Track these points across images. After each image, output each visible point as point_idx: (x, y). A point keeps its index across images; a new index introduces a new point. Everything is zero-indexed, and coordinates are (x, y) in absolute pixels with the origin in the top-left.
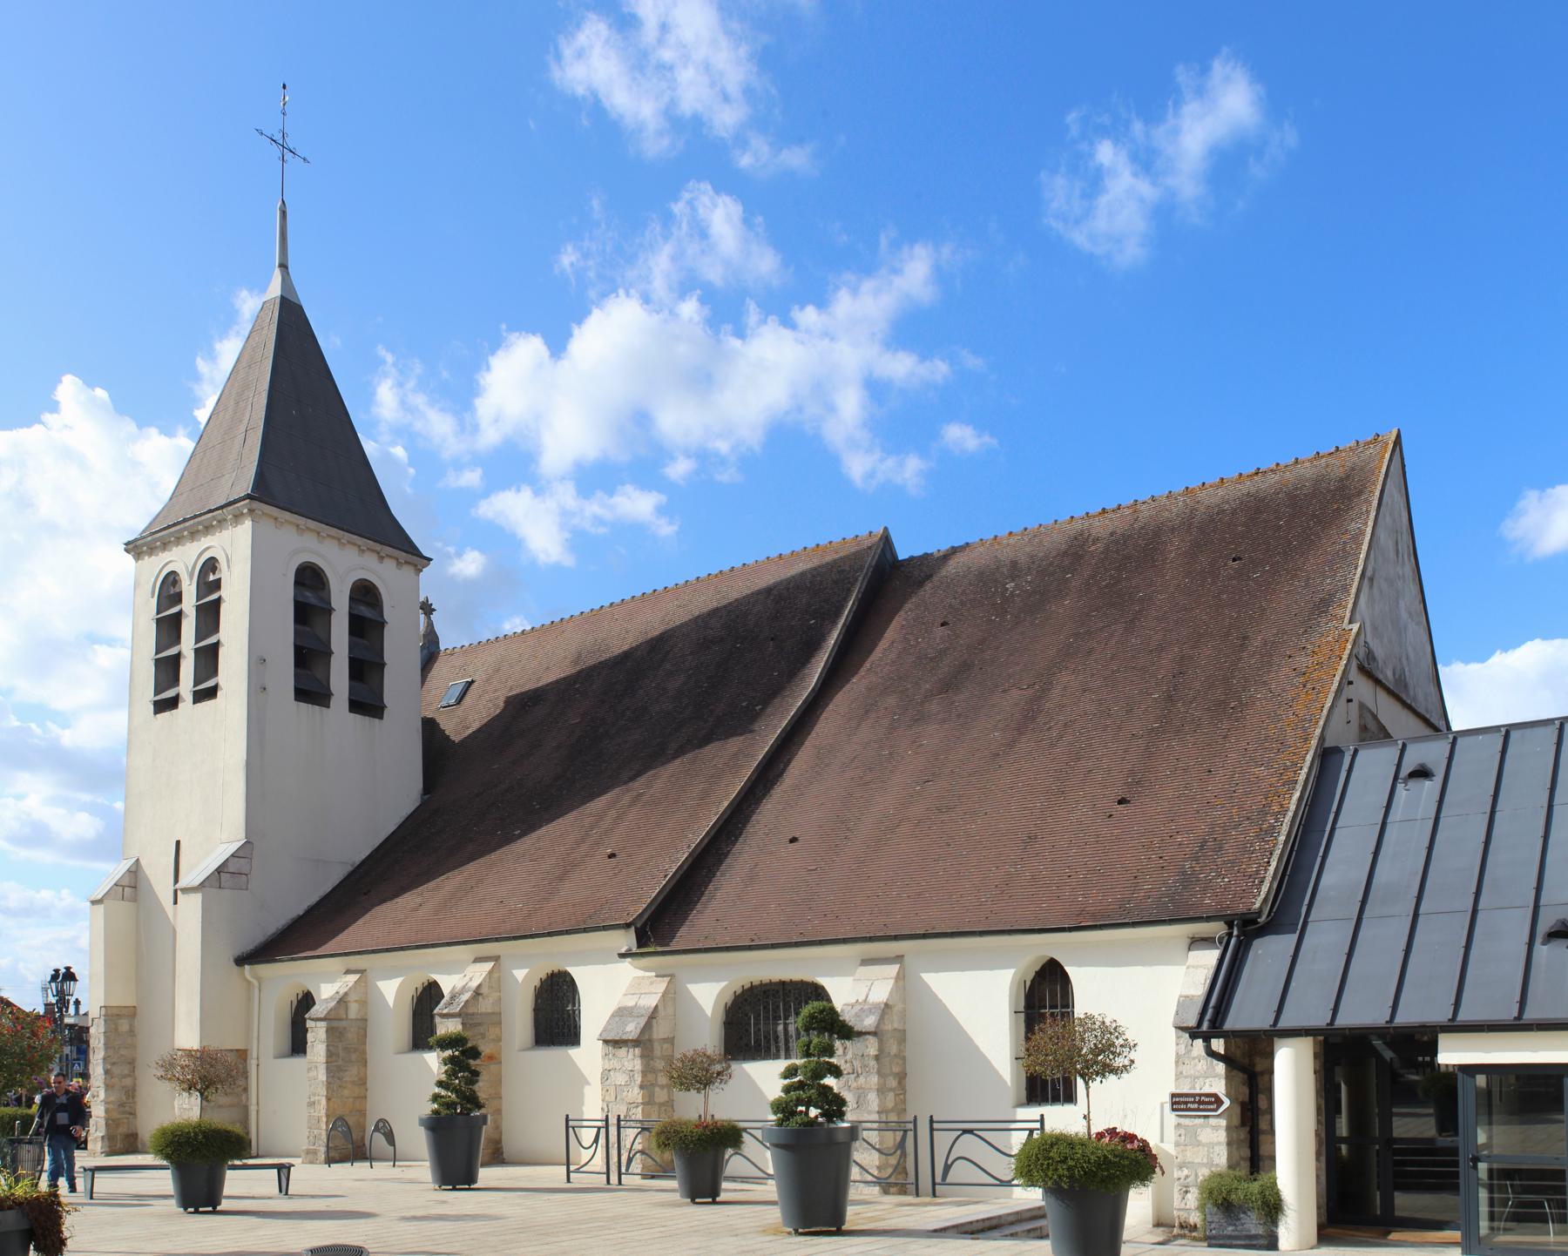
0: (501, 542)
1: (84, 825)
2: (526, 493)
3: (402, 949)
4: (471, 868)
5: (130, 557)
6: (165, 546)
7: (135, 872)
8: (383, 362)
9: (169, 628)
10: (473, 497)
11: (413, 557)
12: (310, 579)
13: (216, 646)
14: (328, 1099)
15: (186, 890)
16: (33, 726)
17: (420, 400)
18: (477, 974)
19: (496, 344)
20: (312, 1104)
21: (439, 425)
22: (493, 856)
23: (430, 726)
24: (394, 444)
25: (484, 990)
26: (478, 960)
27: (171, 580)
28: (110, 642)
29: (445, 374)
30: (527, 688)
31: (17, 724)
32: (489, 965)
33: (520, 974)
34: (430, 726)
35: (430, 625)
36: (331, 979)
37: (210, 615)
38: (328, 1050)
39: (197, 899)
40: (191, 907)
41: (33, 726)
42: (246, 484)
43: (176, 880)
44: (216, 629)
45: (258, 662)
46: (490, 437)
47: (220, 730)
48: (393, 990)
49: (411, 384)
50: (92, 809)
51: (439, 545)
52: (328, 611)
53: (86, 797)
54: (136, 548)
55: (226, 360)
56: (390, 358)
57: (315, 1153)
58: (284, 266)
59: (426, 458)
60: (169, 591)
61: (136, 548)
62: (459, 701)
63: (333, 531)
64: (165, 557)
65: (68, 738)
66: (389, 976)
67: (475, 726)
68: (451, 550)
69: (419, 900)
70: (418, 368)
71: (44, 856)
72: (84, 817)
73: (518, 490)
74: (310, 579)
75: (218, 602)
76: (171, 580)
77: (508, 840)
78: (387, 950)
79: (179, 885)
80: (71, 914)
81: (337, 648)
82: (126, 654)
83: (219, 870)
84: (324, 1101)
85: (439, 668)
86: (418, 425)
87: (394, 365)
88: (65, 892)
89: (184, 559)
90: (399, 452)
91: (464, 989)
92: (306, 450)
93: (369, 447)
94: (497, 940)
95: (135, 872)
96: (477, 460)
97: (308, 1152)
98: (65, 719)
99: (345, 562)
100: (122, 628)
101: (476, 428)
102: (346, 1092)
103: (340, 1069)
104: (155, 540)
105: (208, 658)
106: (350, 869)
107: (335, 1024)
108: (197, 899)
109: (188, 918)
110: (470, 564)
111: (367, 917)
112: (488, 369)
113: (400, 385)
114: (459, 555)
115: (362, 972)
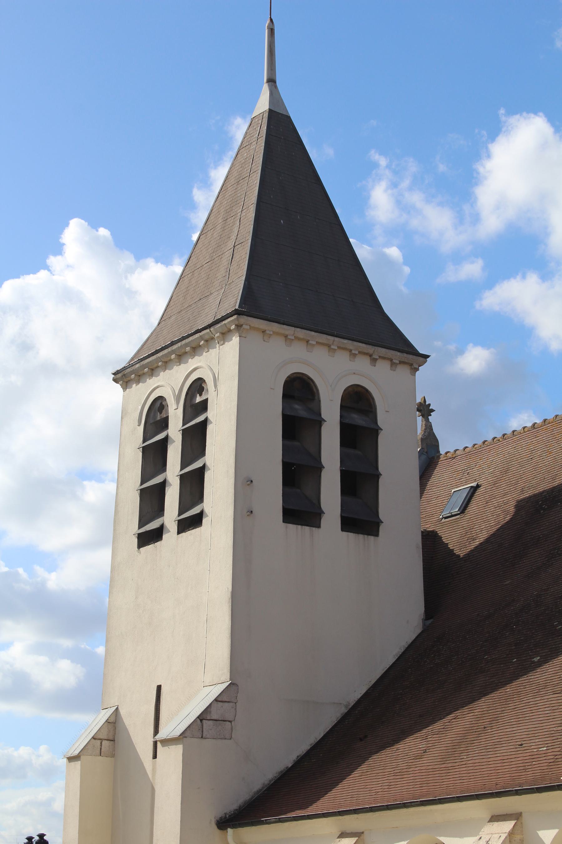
0: (509, 332)
1: (64, 673)
2: (533, 279)
3: (405, 806)
4: (483, 704)
5: (118, 387)
6: (153, 371)
7: (114, 723)
8: (376, 165)
9: (154, 456)
10: (474, 289)
11: (408, 355)
12: (299, 391)
13: (202, 470)
15: (167, 742)
16: (21, 570)
17: (416, 198)
19: (495, 130)
21: (437, 220)
22: (509, 689)
23: (430, 540)
24: (388, 244)
26: (496, 818)
27: (158, 405)
28: (97, 477)
29: (442, 168)
30: (540, 489)
31: (6, 569)
32: (508, 826)
34: (430, 540)
35: (429, 428)
37: (196, 438)
39: (177, 751)
40: (172, 759)
41: (21, 570)
42: (233, 301)
43: (156, 731)
44: (202, 452)
45: (244, 483)
46: (491, 224)
47: (204, 560)
49: (406, 183)
50: (74, 655)
51: (438, 344)
52: (319, 422)
53: (67, 643)
54: (125, 377)
55: (217, 180)
56: (383, 162)
58: (272, 81)
59: (424, 256)
61: (125, 377)
62: (464, 509)
63: (324, 338)
64: (151, 383)
65: (54, 581)
67: (483, 536)
68: (452, 347)
69: (423, 746)
70: (413, 167)
71: (23, 710)
72: (65, 664)
73: (524, 277)
75: (205, 423)
76: (158, 405)
77: (526, 668)
79: (162, 735)
80: (47, 773)
81: (329, 463)
82: (112, 487)
83: (201, 718)
85: (440, 475)
86: (415, 223)
87: (388, 167)
88: (43, 749)
90: (394, 252)
92: (296, 259)
93: (363, 252)
94: (517, 793)
95: (114, 723)
96: (480, 250)
98: (51, 562)
99: (334, 369)
100: (110, 463)
101: (476, 219)
104: (144, 367)
105: (193, 485)
106: (344, 710)
108: (177, 751)
109: (167, 774)
110: (474, 360)
112: (489, 156)
113: (394, 185)
114: (461, 352)
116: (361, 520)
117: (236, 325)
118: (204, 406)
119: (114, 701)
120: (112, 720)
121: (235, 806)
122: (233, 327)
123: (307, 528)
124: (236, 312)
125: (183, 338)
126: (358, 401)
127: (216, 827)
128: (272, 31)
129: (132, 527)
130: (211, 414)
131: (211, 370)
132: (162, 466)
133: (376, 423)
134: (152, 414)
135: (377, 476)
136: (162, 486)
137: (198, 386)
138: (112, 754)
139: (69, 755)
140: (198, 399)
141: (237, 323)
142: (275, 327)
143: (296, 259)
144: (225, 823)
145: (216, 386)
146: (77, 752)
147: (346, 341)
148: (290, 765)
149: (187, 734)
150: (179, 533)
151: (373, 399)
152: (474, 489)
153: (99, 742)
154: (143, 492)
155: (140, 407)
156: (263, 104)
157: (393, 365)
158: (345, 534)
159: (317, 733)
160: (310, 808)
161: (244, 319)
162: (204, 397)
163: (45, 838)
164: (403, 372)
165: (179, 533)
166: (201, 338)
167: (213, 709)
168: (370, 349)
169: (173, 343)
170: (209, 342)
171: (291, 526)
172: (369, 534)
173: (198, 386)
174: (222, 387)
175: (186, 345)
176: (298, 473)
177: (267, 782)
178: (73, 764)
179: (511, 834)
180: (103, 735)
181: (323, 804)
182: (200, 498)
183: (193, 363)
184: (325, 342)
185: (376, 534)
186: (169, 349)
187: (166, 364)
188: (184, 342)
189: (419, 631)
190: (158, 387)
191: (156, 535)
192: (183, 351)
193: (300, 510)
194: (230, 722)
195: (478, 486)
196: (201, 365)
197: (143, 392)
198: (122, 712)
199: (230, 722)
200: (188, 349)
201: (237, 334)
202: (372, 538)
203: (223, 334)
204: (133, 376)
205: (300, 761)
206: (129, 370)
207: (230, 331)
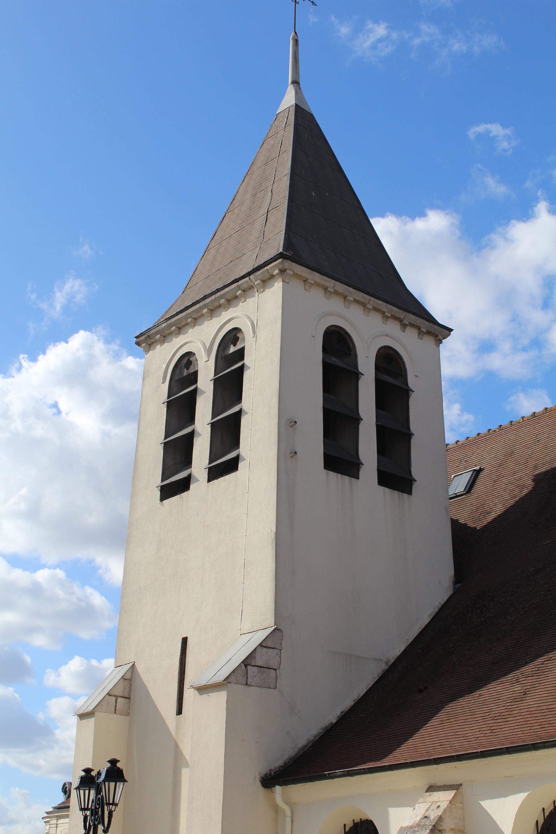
6: (180, 329)
9: (181, 408)
12: (337, 343)
27: (187, 360)
36: (406, 799)
37: (230, 385)
39: (219, 699)
45: (288, 425)
52: (356, 375)
60: (183, 375)
63: (361, 296)
66: (502, 790)
74: (337, 343)
76: (187, 360)
83: (246, 663)
104: (171, 325)
105: (228, 432)
108: (219, 699)
111: (442, 715)
115: (456, 787)
116: (396, 477)
117: (280, 270)
118: (240, 354)
119: (130, 658)
120: (128, 676)
121: (280, 763)
122: (277, 271)
123: (347, 478)
124: (280, 256)
125: (218, 290)
126: (390, 362)
127: (259, 784)
128: (296, 42)
129: (155, 479)
130: (247, 360)
131: (249, 318)
133: (407, 385)
134: (178, 371)
135: (409, 435)
136: (191, 437)
137: (233, 335)
138: (128, 714)
139: (81, 712)
140: (232, 349)
141: (281, 267)
142: (316, 277)
144: (270, 781)
145: (254, 332)
146: (90, 708)
147: (380, 302)
148: (334, 721)
149: (232, 679)
150: (209, 481)
151: (403, 363)
153: (114, 698)
154: (167, 446)
155: (164, 366)
156: (289, 99)
157: (421, 333)
158: (381, 488)
160: (391, 756)
161: (288, 264)
162: (239, 346)
163: (118, 765)
164: (429, 341)
165: (209, 481)
166: (239, 288)
167: (258, 654)
168: (401, 314)
169: (205, 297)
170: (247, 291)
172: (403, 491)
173: (233, 335)
174: (262, 334)
175: (221, 297)
176: (338, 422)
177: (311, 738)
178: (85, 721)
180: (119, 692)
181: (400, 755)
182: (236, 443)
183: (225, 315)
184: (362, 300)
185: (410, 492)
186: (201, 304)
187: (196, 320)
188: (218, 294)
189: (450, 593)
190: (185, 344)
191: (184, 485)
192: (216, 304)
193: (340, 460)
194: (275, 670)
195: (481, 470)
197: (166, 354)
198: (140, 668)
199: (275, 670)
200: (222, 301)
201: (280, 279)
202: (406, 496)
203: (264, 281)
204: (158, 336)
206: (154, 331)
207: (273, 276)
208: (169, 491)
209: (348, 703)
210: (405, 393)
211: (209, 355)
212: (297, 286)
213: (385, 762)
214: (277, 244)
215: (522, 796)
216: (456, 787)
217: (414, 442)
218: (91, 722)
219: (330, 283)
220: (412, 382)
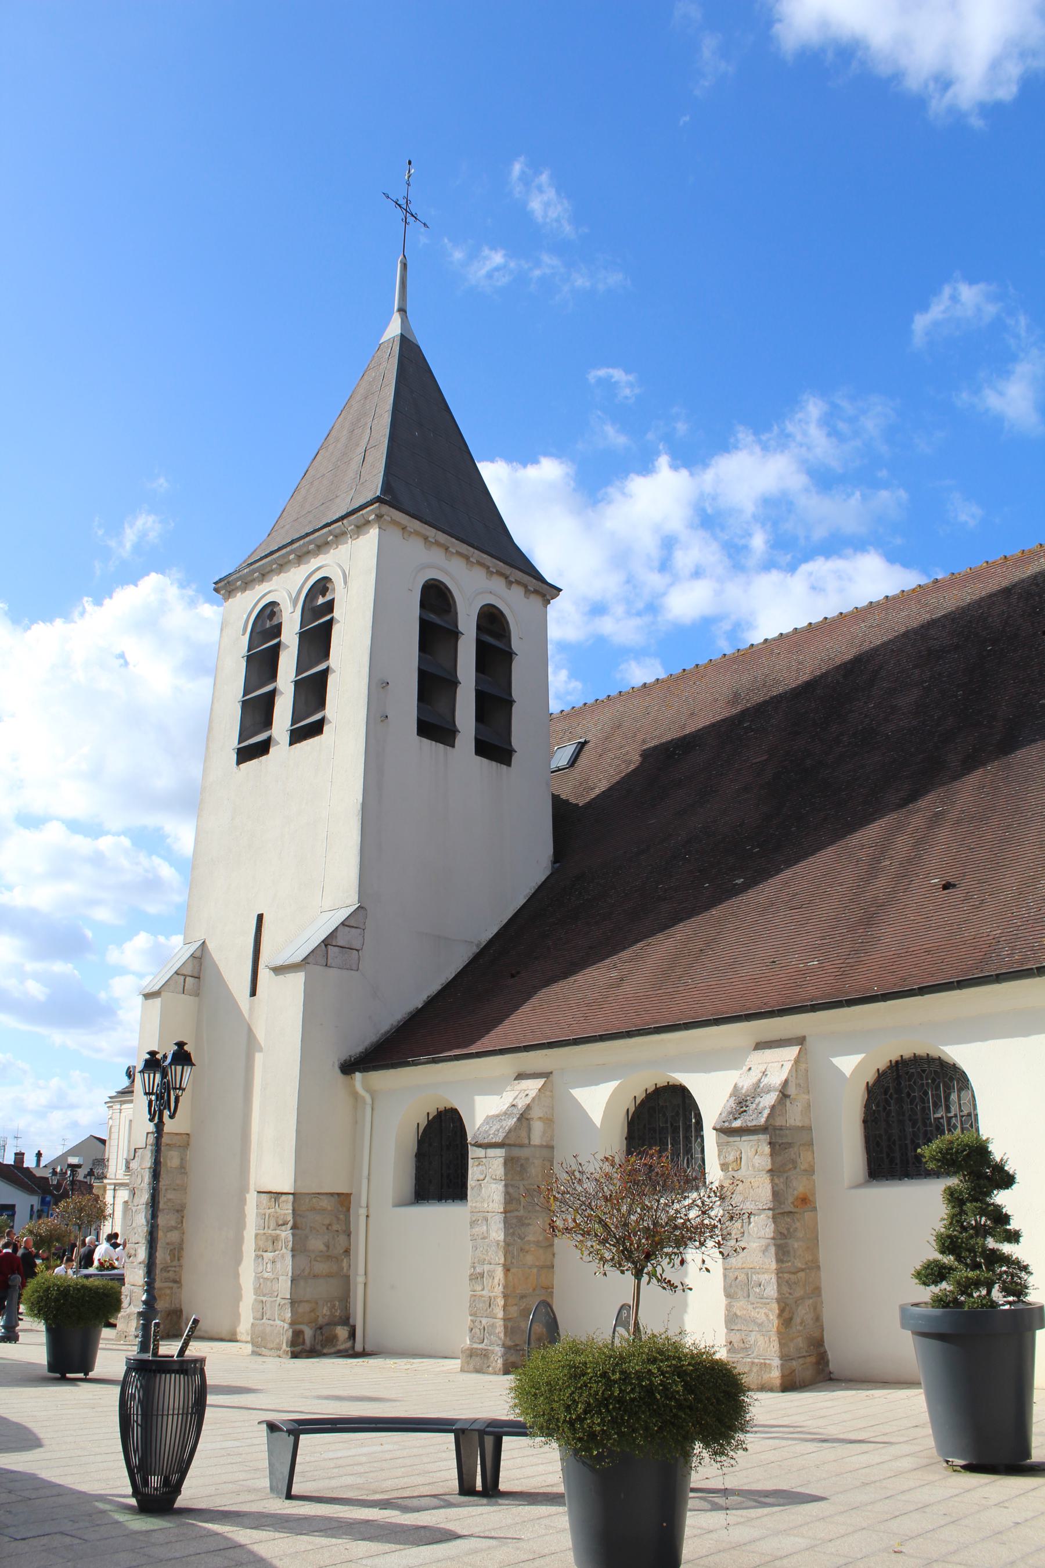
4: (682, 931)
6: (265, 576)
9: (262, 663)
12: (436, 598)
14: (507, 1270)
18: (776, 1067)
20: (477, 1277)
25: (792, 1090)
27: (270, 611)
33: (848, 1064)
36: (494, 1087)
37: (317, 639)
38: (507, 1193)
39: (297, 981)
45: (379, 686)
48: (599, 1100)
57: (485, 1355)
60: (266, 626)
63: (464, 548)
64: (261, 589)
74: (436, 598)
76: (270, 611)
77: (725, 893)
78: (576, 1042)
83: (326, 942)
84: (499, 1273)
89: (286, 590)
91: (757, 1090)
97: (471, 1354)
102: (529, 1259)
103: (522, 1222)
104: (254, 571)
105: (313, 690)
107: (516, 1152)
108: (297, 981)
111: (534, 1001)
115: (546, 1075)
116: (495, 747)
117: (376, 515)
118: (330, 606)
119: (199, 936)
120: (198, 954)
122: (373, 517)
123: (441, 745)
124: (378, 500)
125: (307, 535)
126: (492, 621)
127: (339, 1071)
128: (404, 266)
129: (230, 739)
130: (337, 613)
131: (340, 566)
132: (272, 674)
133: (510, 647)
134: (260, 622)
135: (509, 703)
136: (272, 696)
137: (323, 585)
138: (197, 995)
139: (147, 991)
140: (321, 601)
141: (378, 512)
142: (416, 525)
143: (430, 476)
144: (349, 1067)
145: (345, 583)
146: (157, 988)
147: (485, 556)
148: (420, 1006)
149: (309, 960)
150: (291, 744)
151: (507, 623)
152: (582, 745)
153: (182, 978)
154: (244, 704)
155: (245, 616)
156: (394, 329)
157: (527, 592)
158: (479, 758)
159: (449, 973)
160: (479, 1043)
161: (385, 509)
162: (328, 598)
163: (186, 1048)
164: (535, 601)
165: (291, 744)
166: (330, 533)
167: (339, 934)
169: (292, 542)
170: (340, 537)
171: (426, 742)
172: (501, 763)
173: (323, 585)
174: (354, 584)
175: (310, 542)
177: (395, 1024)
178: (150, 1001)
179: (797, 1061)
180: (187, 971)
182: (321, 704)
183: (315, 563)
184: (465, 553)
185: (509, 764)
186: (288, 549)
187: (282, 567)
188: (307, 539)
189: (548, 873)
190: (269, 592)
191: (263, 748)
192: (305, 550)
193: (435, 728)
194: (358, 950)
195: (586, 742)
196: (326, 564)
197: (246, 604)
198: (210, 945)
199: (358, 950)
200: (312, 547)
201: (377, 526)
203: (358, 527)
204: (239, 583)
205: (432, 1002)
206: (234, 576)
207: (368, 523)
208: (245, 754)
209: (435, 987)
210: (508, 656)
211: (295, 605)
212: (395, 534)
213: (473, 1049)
214: (374, 486)
215: (614, 1084)
216: (546, 1075)
217: (515, 709)
218: (157, 1002)
219: (431, 532)
220: (516, 644)
